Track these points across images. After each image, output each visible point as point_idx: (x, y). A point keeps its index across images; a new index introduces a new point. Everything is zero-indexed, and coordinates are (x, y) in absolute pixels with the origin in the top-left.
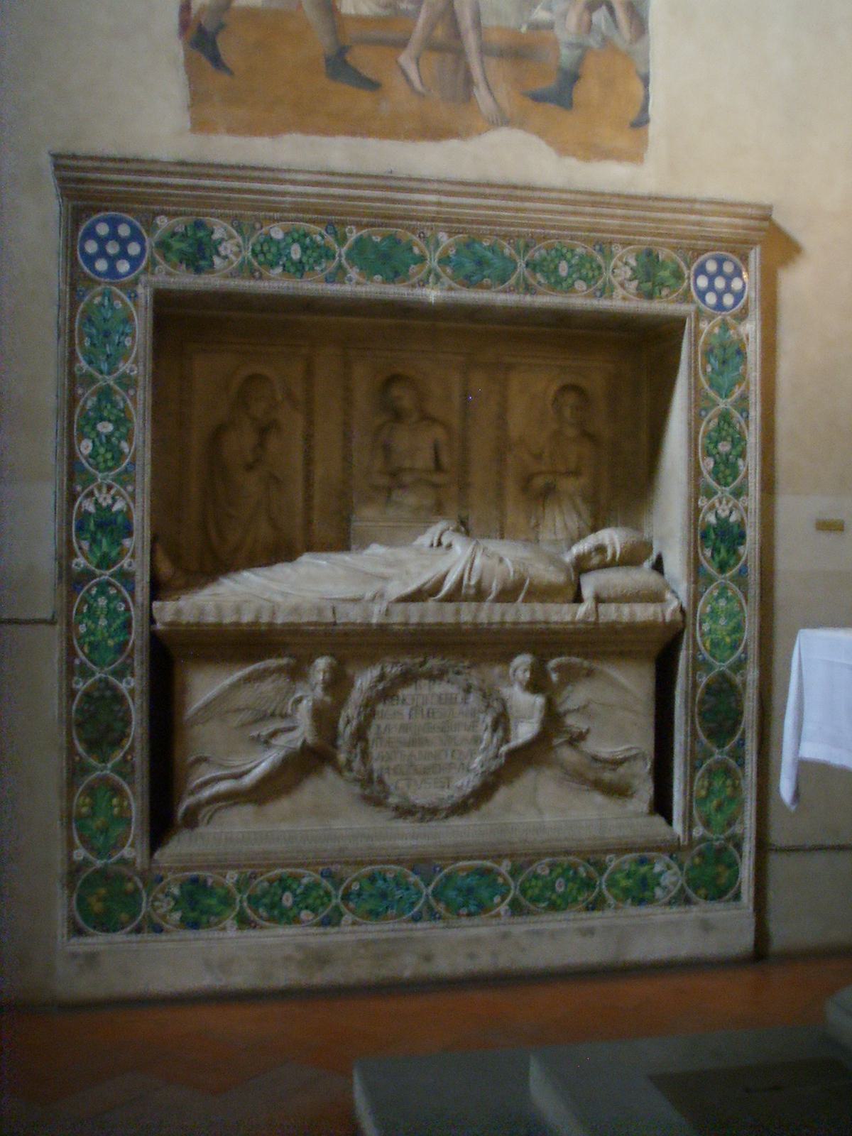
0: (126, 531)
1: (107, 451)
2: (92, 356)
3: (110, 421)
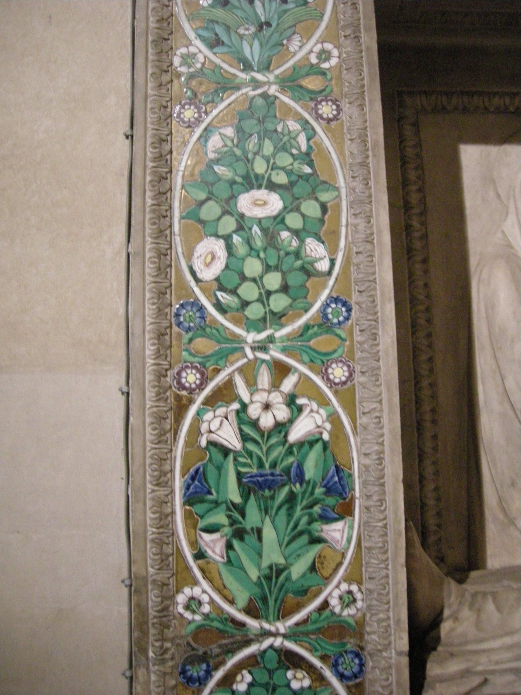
0: (331, 501)
1: (268, 268)
2: (219, 30)
3: (272, 186)
